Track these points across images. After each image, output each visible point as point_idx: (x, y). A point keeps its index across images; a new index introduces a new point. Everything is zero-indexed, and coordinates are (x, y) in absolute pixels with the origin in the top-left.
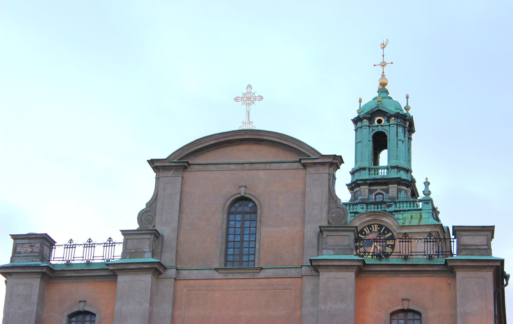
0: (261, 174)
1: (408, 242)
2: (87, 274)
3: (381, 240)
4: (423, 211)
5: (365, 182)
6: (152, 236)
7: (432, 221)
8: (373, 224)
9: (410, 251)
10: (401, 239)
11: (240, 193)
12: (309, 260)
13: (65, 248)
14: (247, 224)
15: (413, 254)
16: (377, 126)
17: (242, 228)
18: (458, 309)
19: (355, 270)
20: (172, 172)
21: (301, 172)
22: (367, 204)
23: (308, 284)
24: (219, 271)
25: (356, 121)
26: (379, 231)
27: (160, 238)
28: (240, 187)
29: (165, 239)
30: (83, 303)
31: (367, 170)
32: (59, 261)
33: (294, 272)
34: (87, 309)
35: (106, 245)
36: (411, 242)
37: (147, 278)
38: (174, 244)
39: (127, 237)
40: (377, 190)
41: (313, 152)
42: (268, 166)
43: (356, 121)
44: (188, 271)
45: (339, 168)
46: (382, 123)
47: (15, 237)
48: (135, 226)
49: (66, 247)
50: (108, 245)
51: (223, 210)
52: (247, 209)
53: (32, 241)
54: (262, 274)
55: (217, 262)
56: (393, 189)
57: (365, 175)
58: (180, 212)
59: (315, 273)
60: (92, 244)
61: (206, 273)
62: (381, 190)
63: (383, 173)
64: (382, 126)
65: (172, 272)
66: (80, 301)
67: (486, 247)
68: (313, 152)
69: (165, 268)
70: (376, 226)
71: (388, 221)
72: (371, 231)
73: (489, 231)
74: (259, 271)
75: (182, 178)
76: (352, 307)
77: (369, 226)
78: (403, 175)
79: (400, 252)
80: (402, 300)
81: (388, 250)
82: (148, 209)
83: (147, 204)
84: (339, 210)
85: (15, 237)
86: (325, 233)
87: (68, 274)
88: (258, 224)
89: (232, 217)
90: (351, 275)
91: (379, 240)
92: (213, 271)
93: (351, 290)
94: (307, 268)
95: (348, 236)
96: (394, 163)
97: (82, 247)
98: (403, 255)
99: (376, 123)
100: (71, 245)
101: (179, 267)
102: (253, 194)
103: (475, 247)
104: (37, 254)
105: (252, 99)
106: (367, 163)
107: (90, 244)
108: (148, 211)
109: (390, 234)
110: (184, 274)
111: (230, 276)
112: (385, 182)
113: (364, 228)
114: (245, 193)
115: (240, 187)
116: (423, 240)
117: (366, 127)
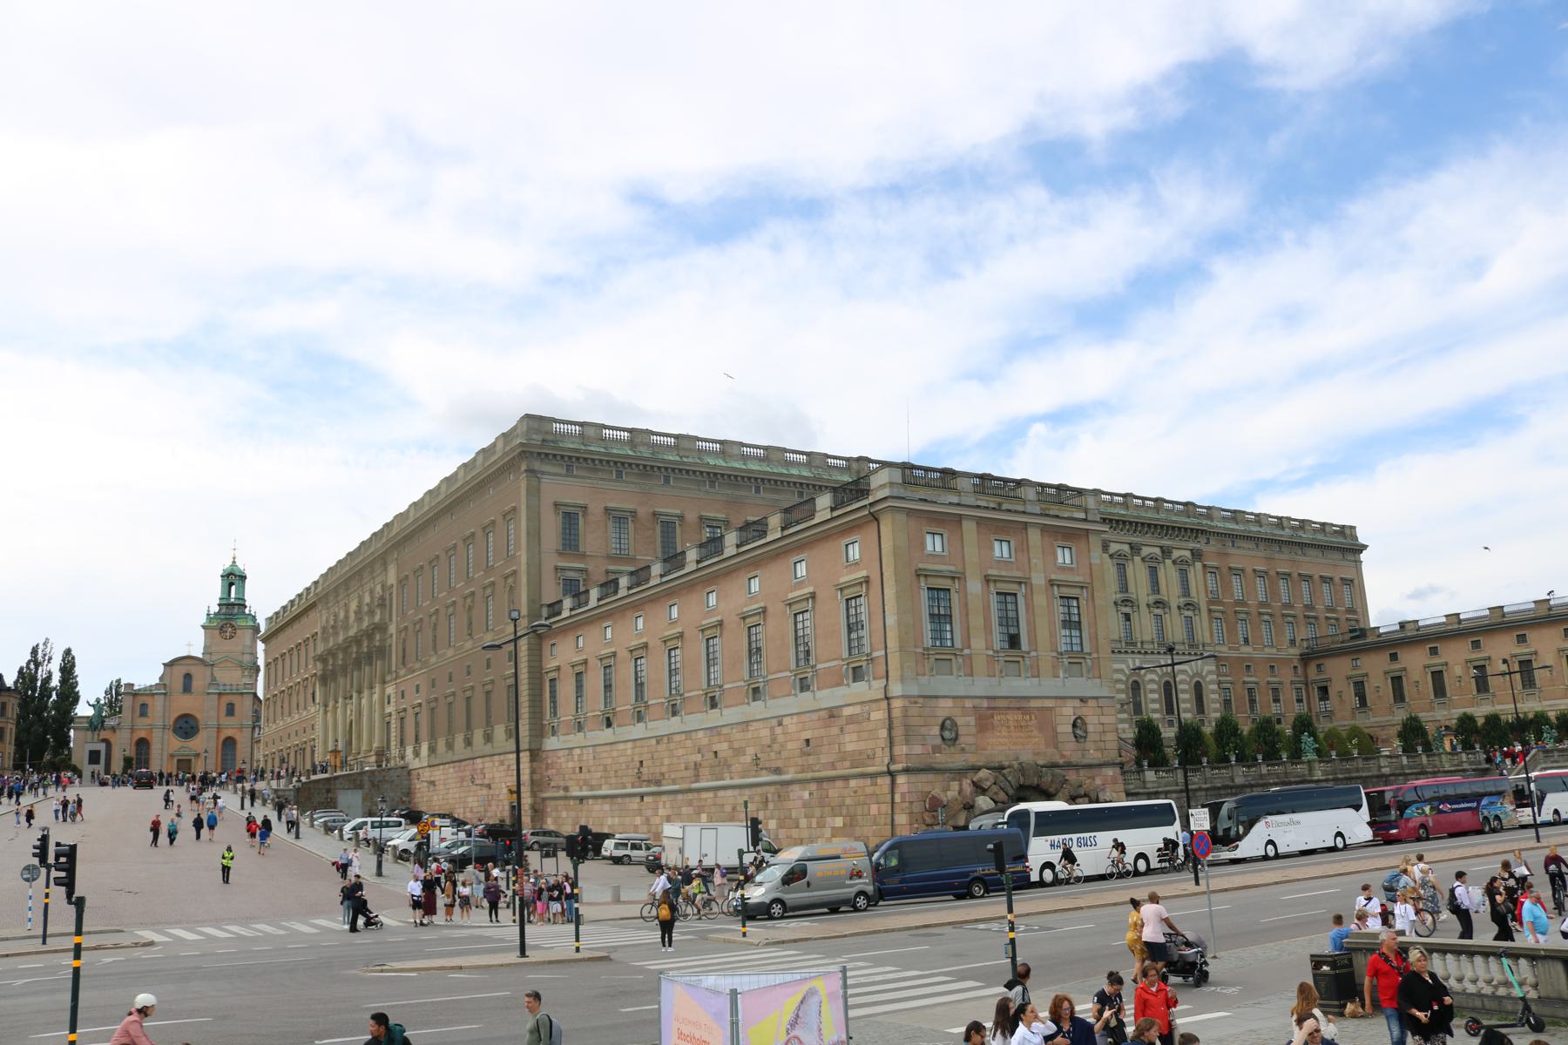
5: (225, 604)
7: (252, 624)
25: (222, 576)
37: (162, 696)
43: (222, 576)
48: (158, 681)
55: (181, 690)
56: (236, 607)
57: (225, 602)
63: (232, 600)
71: (233, 623)
78: (241, 602)
90: (216, 696)
96: (238, 596)
106: (225, 596)
112: (233, 605)
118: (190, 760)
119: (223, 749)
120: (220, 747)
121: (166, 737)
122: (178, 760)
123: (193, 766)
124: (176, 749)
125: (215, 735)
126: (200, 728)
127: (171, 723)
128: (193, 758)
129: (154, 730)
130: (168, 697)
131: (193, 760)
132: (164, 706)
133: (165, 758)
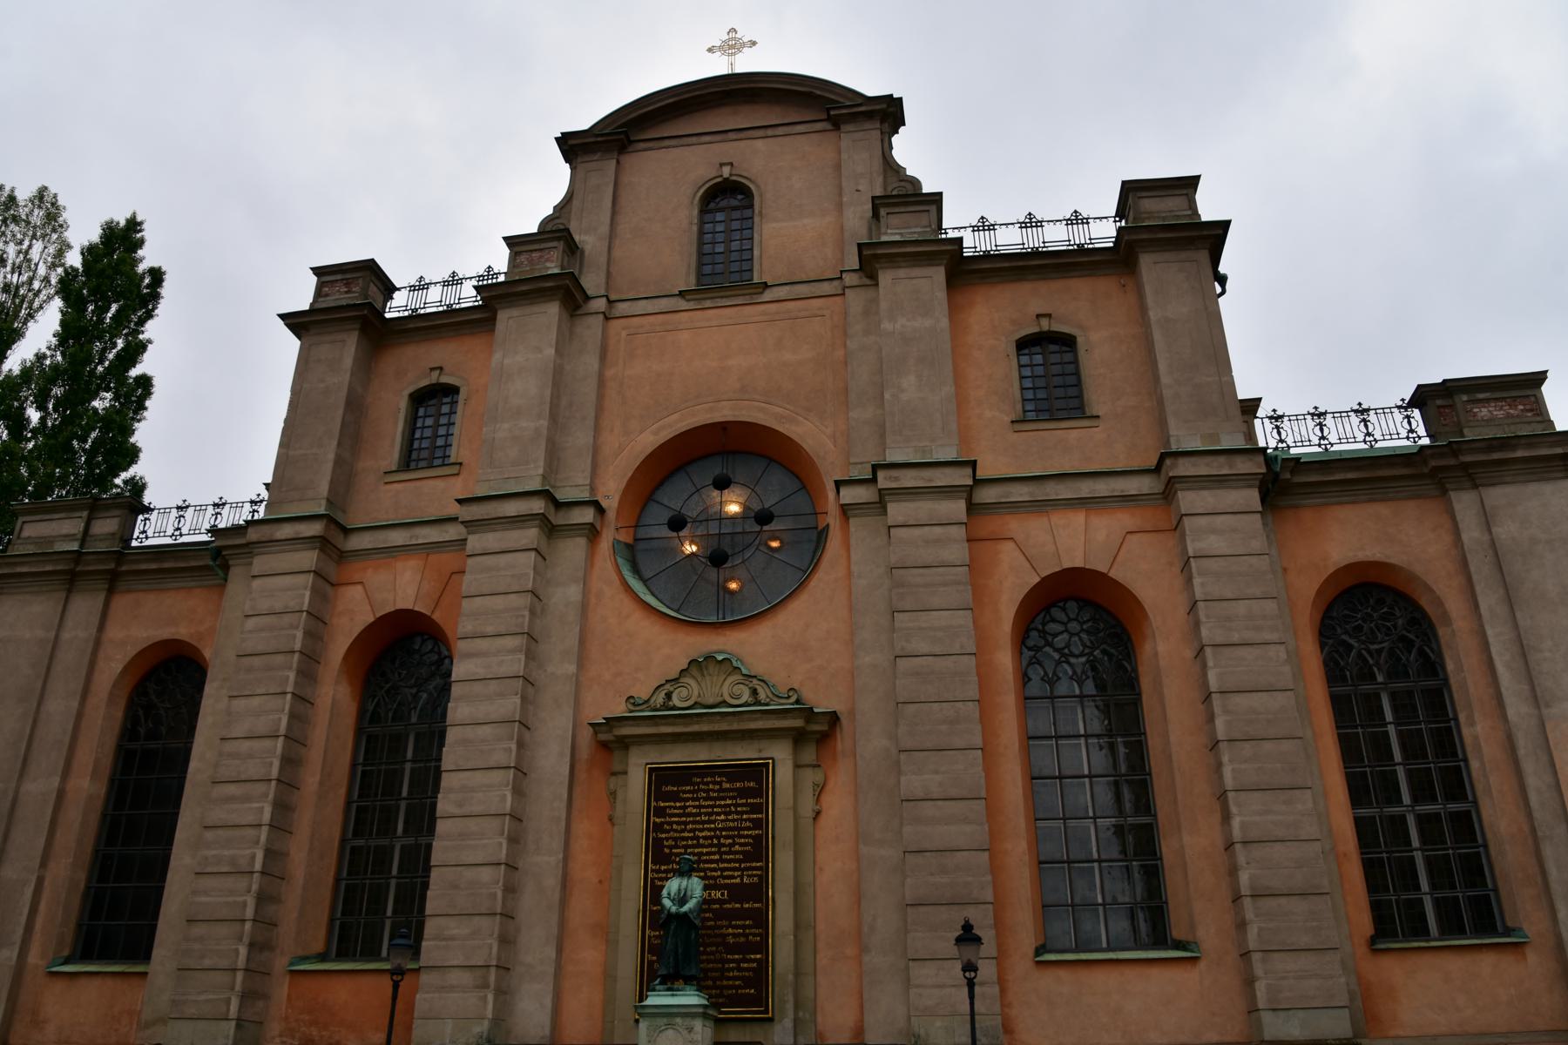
0: (759, 144)
1: (1037, 226)
2: (445, 321)
3: (986, 228)
6: (562, 242)
9: (1041, 240)
10: (1023, 223)
11: (721, 176)
13: (410, 291)
14: (736, 225)
15: (1046, 245)
17: (729, 231)
18: (1151, 314)
19: (945, 262)
20: (599, 154)
21: (832, 136)
23: (855, 300)
24: (687, 297)
27: (578, 254)
28: (722, 165)
29: (587, 253)
30: (438, 372)
32: (399, 311)
33: (826, 288)
34: (445, 379)
35: (481, 278)
36: (1042, 226)
38: (603, 260)
39: (517, 249)
41: (850, 95)
42: (770, 132)
44: (628, 303)
45: (897, 133)
47: (317, 271)
49: (413, 288)
50: (486, 278)
51: (692, 203)
52: (734, 203)
53: (348, 276)
54: (768, 295)
58: (614, 213)
59: (868, 282)
60: (457, 280)
61: (664, 304)
65: (600, 304)
66: (432, 369)
67: (1189, 212)
68: (850, 95)
69: (587, 298)
73: (1192, 182)
74: (761, 290)
75: (618, 162)
76: (944, 322)
79: (1023, 244)
80: (1038, 316)
82: (558, 214)
83: (555, 207)
84: (903, 184)
85: (317, 271)
86: (883, 212)
87: (411, 326)
88: (756, 219)
89: (708, 217)
91: (981, 228)
92: (676, 299)
93: (941, 294)
94: (852, 274)
95: (927, 213)
97: (439, 287)
98: (1029, 248)
100: (421, 286)
101: (613, 297)
102: (745, 174)
103: (1168, 214)
104: (357, 295)
105: (738, 46)
107: (454, 281)
108: (557, 218)
110: (622, 308)
111: (708, 304)
114: (731, 175)
115: (722, 165)
116: (1065, 222)
118: (757, 774)
119: (1026, 699)
120: (1005, 660)
121: (565, 595)
122: (663, 781)
123: (782, 828)
124: (642, 692)
125: (957, 551)
126: (833, 519)
127: (611, 492)
128: (780, 755)
129: (475, 542)
130: (591, 328)
131: (783, 774)
132: (558, 379)
133: (552, 761)
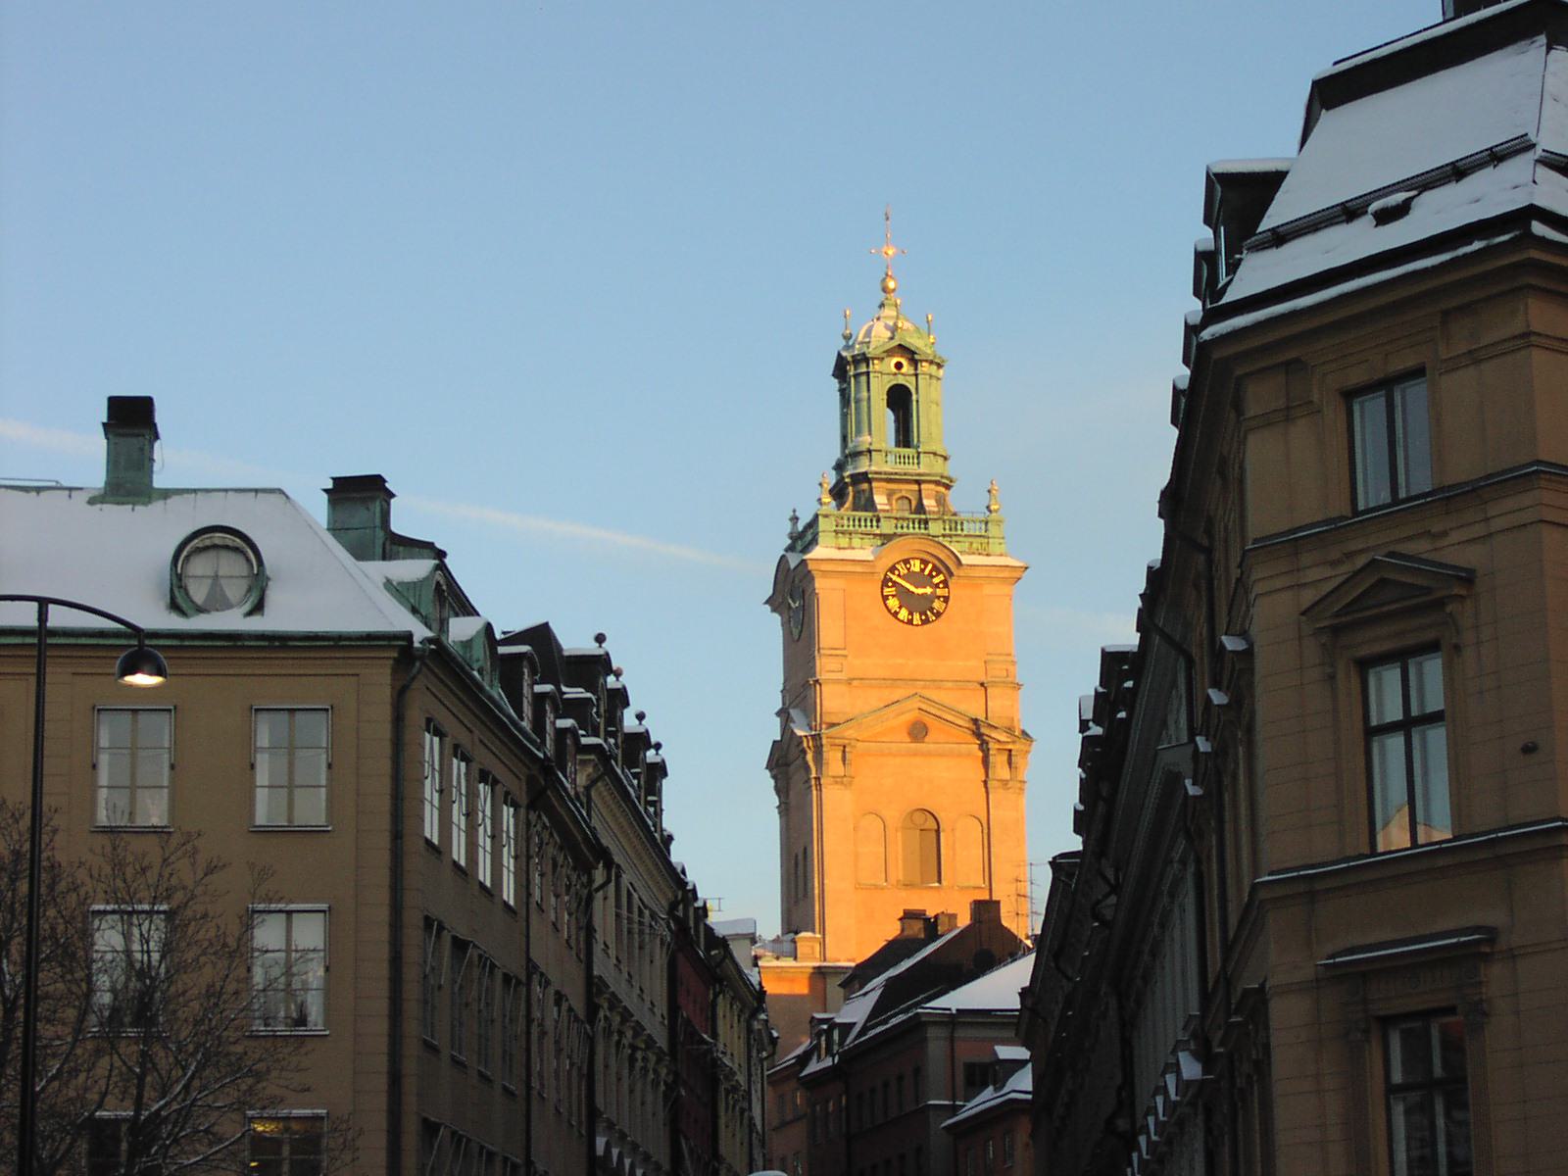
4: (991, 540)
8: (913, 558)
12: (394, 491)
16: (895, 374)
22: (896, 519)
26: (923, 570)
31: (884, 454)
40: (901, 491)
46: (904, 370)
62: (907, 490)
64: (903, 374)
70: (918, 562)
72: (909, 569)
77: (906, 561)
81: (937, 605)
99: (894, 370)
109: (941, 577)
113: (898, 563)
117: (876, 374)
